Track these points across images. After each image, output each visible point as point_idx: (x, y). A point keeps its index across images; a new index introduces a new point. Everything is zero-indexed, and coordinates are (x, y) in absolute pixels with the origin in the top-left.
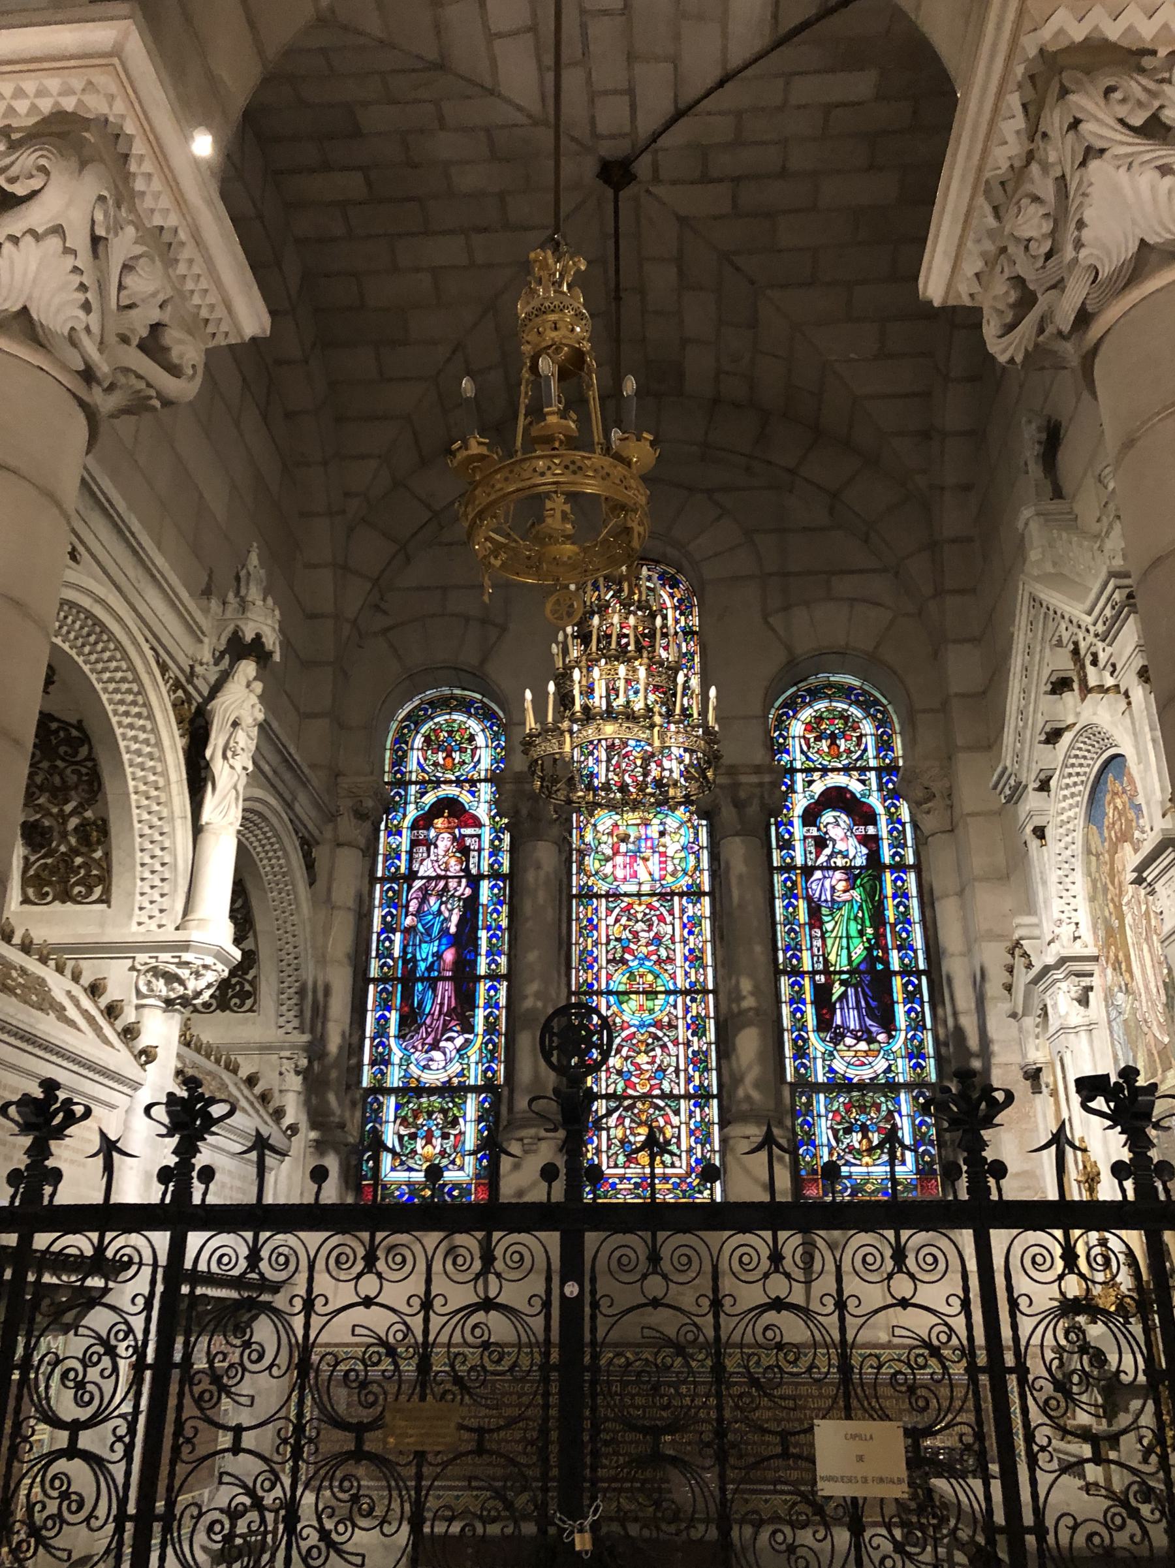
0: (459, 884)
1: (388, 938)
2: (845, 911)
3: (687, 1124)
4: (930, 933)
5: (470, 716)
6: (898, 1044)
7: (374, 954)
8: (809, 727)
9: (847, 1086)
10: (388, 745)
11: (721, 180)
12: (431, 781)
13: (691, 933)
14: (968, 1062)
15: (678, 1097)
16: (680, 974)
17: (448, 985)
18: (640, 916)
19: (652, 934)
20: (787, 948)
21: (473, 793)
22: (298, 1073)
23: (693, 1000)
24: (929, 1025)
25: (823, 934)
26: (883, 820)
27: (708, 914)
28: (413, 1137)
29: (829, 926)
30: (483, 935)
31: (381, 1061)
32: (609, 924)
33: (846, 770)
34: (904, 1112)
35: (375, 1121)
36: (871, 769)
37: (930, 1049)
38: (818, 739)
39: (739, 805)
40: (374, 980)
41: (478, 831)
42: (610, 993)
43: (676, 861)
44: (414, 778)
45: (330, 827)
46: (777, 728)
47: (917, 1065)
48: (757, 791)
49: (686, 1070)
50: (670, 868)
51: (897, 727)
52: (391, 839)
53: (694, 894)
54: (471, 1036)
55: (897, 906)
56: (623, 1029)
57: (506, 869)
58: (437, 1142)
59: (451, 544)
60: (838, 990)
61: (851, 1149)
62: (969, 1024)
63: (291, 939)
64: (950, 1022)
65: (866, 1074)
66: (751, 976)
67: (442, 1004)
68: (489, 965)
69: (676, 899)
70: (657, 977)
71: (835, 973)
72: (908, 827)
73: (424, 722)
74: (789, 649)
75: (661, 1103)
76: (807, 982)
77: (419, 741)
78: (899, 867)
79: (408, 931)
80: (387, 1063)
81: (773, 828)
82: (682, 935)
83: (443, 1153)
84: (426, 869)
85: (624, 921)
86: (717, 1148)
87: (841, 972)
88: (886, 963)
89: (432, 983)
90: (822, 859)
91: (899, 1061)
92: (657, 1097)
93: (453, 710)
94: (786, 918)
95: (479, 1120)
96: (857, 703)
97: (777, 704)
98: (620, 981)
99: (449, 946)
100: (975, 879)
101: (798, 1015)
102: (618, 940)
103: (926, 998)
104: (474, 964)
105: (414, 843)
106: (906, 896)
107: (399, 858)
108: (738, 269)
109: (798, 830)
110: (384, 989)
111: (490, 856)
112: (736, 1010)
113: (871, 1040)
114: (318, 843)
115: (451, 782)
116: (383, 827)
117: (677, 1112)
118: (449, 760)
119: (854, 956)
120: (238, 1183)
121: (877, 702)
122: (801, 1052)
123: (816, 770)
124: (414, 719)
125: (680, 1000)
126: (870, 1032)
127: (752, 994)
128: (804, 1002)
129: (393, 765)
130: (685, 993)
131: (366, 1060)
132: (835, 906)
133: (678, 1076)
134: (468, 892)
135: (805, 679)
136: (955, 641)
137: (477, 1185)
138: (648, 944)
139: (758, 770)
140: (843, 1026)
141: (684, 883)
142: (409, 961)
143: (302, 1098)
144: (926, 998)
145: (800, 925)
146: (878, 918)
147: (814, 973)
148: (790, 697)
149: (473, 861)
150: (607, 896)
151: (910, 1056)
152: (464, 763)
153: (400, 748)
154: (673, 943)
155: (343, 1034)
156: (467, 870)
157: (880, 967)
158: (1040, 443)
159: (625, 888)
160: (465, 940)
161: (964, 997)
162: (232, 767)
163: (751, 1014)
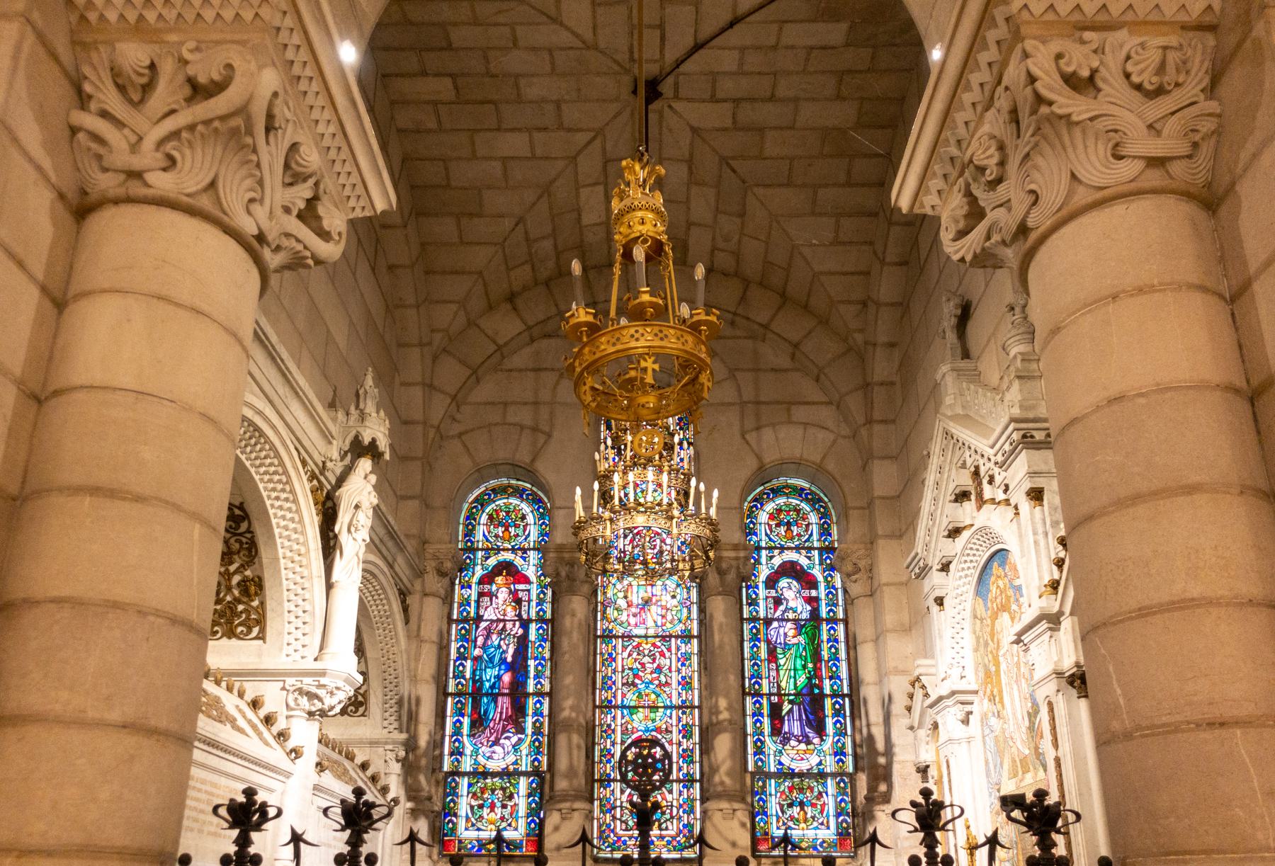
1: (462, 664)
3: (678, 800)
5: (522, 500)
6: (828, 745)
7: (451, 675)
8: (772, 517)
9: (792, 774)
10: (461, 520)
12: (492, 549)
13: (683, 665)
16: (675, 694)
18: (646, 652)
19: (655, 665)
20: (752, 677)
21: (524, 559)
22: (398, 761)
23: (684, 713)
24: (849, 733)
25: (777, 667)
26: (822, 586)
27: (696, 652)
28: (481, 806)
29: (782, 662)
30: (531, 663)
31: (458, 753)
32: (624, 658)
33: (797, 549)
34: (830, 793)
35: (453, 795)
36: (815, 549)
37: (849, 750)
38: (778, 525)
39: (721, 573)
40: (451, 694)
42: (624, 707)
43: (674, 613)
44: (480, 546)
46: (749, 516)
48: (734, 563)
49: (678, 762)
50: (669, 617)
53: (686, 637)
54: (523, 736)
55: (830, 648)
56: (633, 733)
57: (548, 615)
58: (498, 810)
59: (511, 370)
60: (786, 707)
61: (792, 818)
62: (878, 733)
64: (865, 731)
65: (802, 766)
66: (727, 696)
67: (501, 713)
68: (536, 685)
69: (673, 640)
70: (658, 696)
71: (785, 695)
72: (840, 591)
73: (488, 504)
74: (759, 458)
76: (765, 701)
77: (484, 518)
78: (833, 621)
79: (476, 659)
80: (461, 754)
81: (744, 590)
83: (502, 819)
84: (489, 614)
85: (635, 655)
86: (698, 816)
87: (789, 695)
88: (821, 687)
89: (494, 698)
90: (778, 613)
93: (510, 495)
95: (529, 795)
96: (807, 500)
97: (749, 499)
98: (631, 699)
100: (887, 631)
101: (758, 724)
102: (629, 669)
104: (524, 684)
105: (481, 595)
106: (836, 641)
107: (469, 604)
109: (762, 592)
112: (715, 721)
113: (808, 742)
115: (508, 550)
116: (457, 582)
117: (671, 792)
118: (507, 533)
119: (799, 683)
121: (820, 500)
122: (759, 751)
123: (776, 548)
124: (481, 502)
125: (674, 713)
127: (727, 709)
129: (466, 535)
130: (679, 707)
132: (786, 647)
134: (521, 632)
135: (770, 481)
137: (527, 841)
138: (652, 673)
139: (736, 547)
141: (679, 628)
142: (477, 682)
143: (401, 778)
144: (848, 713)
146: (817, 657)
147: (770, 694)
148: (759, 494)
149: (524, 609)
150: (623, 637)
151: (836, 754)
152: (517, 536)
153: (470, 523)
154: (670, 671)
155: (430, 735)
156: (519, 615)
157: (816, 691)
159: (636, 631)
160: (518, 667)
161: (875, 714)
163: (726, 723)
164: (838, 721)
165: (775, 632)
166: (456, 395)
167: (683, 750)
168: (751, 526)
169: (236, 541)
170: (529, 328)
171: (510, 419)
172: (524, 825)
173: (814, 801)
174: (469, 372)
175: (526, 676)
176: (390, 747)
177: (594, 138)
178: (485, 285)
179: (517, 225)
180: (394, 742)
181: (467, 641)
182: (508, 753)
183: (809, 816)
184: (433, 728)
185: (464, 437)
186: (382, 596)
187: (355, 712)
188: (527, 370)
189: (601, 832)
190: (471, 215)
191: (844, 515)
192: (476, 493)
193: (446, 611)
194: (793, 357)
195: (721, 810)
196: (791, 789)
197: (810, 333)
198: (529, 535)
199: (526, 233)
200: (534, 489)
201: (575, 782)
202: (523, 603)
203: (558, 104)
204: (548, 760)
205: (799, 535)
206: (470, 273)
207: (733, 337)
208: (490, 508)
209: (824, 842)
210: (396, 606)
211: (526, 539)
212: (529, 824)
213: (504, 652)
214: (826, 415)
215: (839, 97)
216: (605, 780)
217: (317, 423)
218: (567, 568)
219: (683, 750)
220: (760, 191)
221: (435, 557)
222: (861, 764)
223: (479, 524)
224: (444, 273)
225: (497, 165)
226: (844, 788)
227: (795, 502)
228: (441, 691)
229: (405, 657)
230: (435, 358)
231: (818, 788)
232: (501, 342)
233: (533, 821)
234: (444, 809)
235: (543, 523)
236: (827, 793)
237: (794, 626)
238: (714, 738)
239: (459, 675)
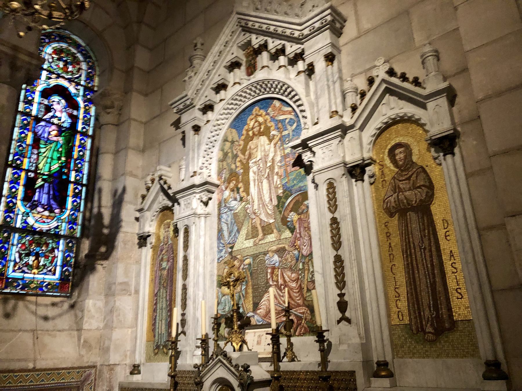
2: (53, 145)
20: (16, 154)
26: (82, 111)
29: (43, 150)
33: (70, 80)
37: (80, 221)
38: (59, 59)
47: (72, 228)
51: (98, 73)
55: (80, 151)
60: (39, 182)
61: (27, 264)
64: (95, 210)
65: (45, 227)
71: (40, 173)
76: (23, 174)
87: (44, 175)
88: (68, 175)
91: (64, 224)
113: (51, 211)
123: (53, 73)
128: (18, 184)
132: (48, 141)
146: (69, 154)
151: (69, 223)
157: (64, 177)
161: (107, 200)
173: (47, 254)
183: (41, 264)
196: (31, 243)
222: (86, 232)
227: (74, 50)
236: (58, 249)
237: (57, 129)
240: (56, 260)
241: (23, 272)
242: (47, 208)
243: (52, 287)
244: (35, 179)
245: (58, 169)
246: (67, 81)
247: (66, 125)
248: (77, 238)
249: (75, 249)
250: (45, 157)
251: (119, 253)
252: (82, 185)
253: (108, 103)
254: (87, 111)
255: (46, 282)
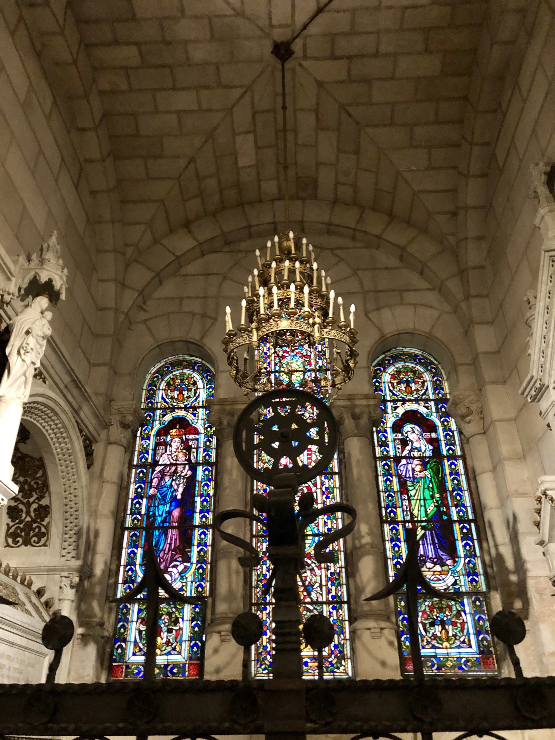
0: (184, 469)
2: (421, 483)
4: (475, 496)
5: (194, 370)
6: (460, 567)
7: (129, 512)
8: (393, 377)
10: (145, 387)
11: (341, 58)
12: (169, 408)
13: (327, 497)
14: (508, 576)
15: (322, 603)
17: (175, 532)
20: (388, 507)
21: (194, 415)
22: (72, 587)
24: (478, 554)
25: (409, 497)
26: (440, 429)
27: (338, 486)
29: (412, 493)
30: (198, 500)
33: (417, 401)
34: (467, 611)
35: (124, 621)
36: (431, 400)
37: (480, 570)
38: (399, 383)
39: (355, 417)
40: (128, 529)
41: (197, 437)
44: (159, 406)
45: (105, 431)
47: (473, 580)
48: (366, 410)
49: (326, 585)
51: (445, 377)
52: (143, 442)
54: (188, 565)
57: (213, 459)
59: (186, 275)
60: (420, 533)
61: (435, 637)
62: (506, 552)
63: (73, 498)
64: (493, 551)
66: (367, 523)
67: (170, 544)
68: (201, 518)
72: (455, 433)
73: (167, 374)
74: (380, 330)
75: (311, 607)
76: (400, 528)
77: (163, 385)
78: (452, 457)
79: (151, 498)
81: (375, 434)
82: (322, 499)
84: (164, 460)
86: (348, 637)
87: (422, 521)
88: (448, 514)
89: (165, 531)
90: (405, 453)
91: (462, 577)
92: (308, 603)
93: (185, 367)
94: (386, 488)
95: (193, 620)
96: (420, 363)
99: (176, 507)
100: (504, 459)
101: (396, 549)
103: (475, 537)
104: (192, 518)
105: (157, 444)
106: (457, 474)
107: (148, 453)
108: (350, 115)
109: (390, 436)
110: (134, 535)
111: (204, 452)
112: (358, 545)
113: (443, 564)
114: (97, 442)
115: (181, 408)
116: (138, 434)
119: (429, 512)
120: (17, 666)
121: (431, 363)
123: (399, 400)
124: (161, 373)
126: (442, 559)
127: (369, 534)
128: (399, 540)
131: (121, 580)
132: (415, 480)
133: (321, 589)
134: (189, 473)
135: (389, 351)
136: (479, 323)
139: (366, 397)
140: (426, 555)
143: (74, 604)
144: (475, 537)
145: (394, 492)
146: (442, 488)
147: (405, 522)
148: (382, 360)
149: (193, 454)
151: (468, 574)
152: (189, 397)
153: (152, 389)
155: (106, 563)
156: (189, 460)
157: (445, 518)
158: (545, 174)
162: (23, 360)
163: (368, 547)
164: (467, 544)
165: (404, 467)
166: (142, 291)
167: (331, 573)
168: (377, 384)
169: (35, 483)
170: (200, 244)
171: (185, 308)
172: (187, 648)
173: (453, 620)
174: (152, 275)
175: (193, 512)
176: (65, 574)
177: (245, 93)
178: (166, 212)
179: (189, 163)
180: (69, 569)
181: (144, 482)
182: (175, 580)
183: (450, 634)
184: (109, 559)
185: (147, 323)
186: (64, 435)
187: (37, 543)
188: (198, 275)
189: (259, 654)
190: (156, 157)
191: (453, 371)
192: (158, 366)
193: (127, 460)
194: (401, 259)
195: (369, 629)
196: (431, 608)
197: (413, 239)
198: (199, 396)
199: (197, 170)
200: (203, 362)
201: (234, 605)
202: (193, 450)
203: (217, 66)
204: (211, 585)
205: (417, 390)
206: (156, 201)
207: (354, 248)
208: (168, 377)
209: (467, 661)
210: (78, 446)
211: (196, 399)
212: (192, 647)
213: (175, 491)
214: (432, 297)
215: (428, 51)
216: (261, 604)
217: (91, 405)
218: (228, 418)
219: (331, 573)
220: (370, 130)
221: (119, 412)
222: (492, 583)
223: (159, 389)
224: (135, 202)
225: (174, 117)
226: (481, 606)
227: (411, 365)
228: (119, 525)
229: (85, 493)
230: (127, 266)
231: (456, 607)
232: (178, 254)
233: (196, 645)
234: (115, 634)
235: (210, 387)
236: (464, 612)
237: (420, 463)
238: (359, 560)
239: (136, 512)
240: (466, 627)
241: (434, 647)
242: (437, 562)
243: (473, 665)
244: (414, 529)
245: (435, 509)
246: (414, 402)
247: (428, 454)
248: (484, 593)
249: (485, 608)
250: (417, 500)
251: (536, 608)
252: (469, 522)
253: (464, 411)
254: (447, 427)
255: (463, 658)
